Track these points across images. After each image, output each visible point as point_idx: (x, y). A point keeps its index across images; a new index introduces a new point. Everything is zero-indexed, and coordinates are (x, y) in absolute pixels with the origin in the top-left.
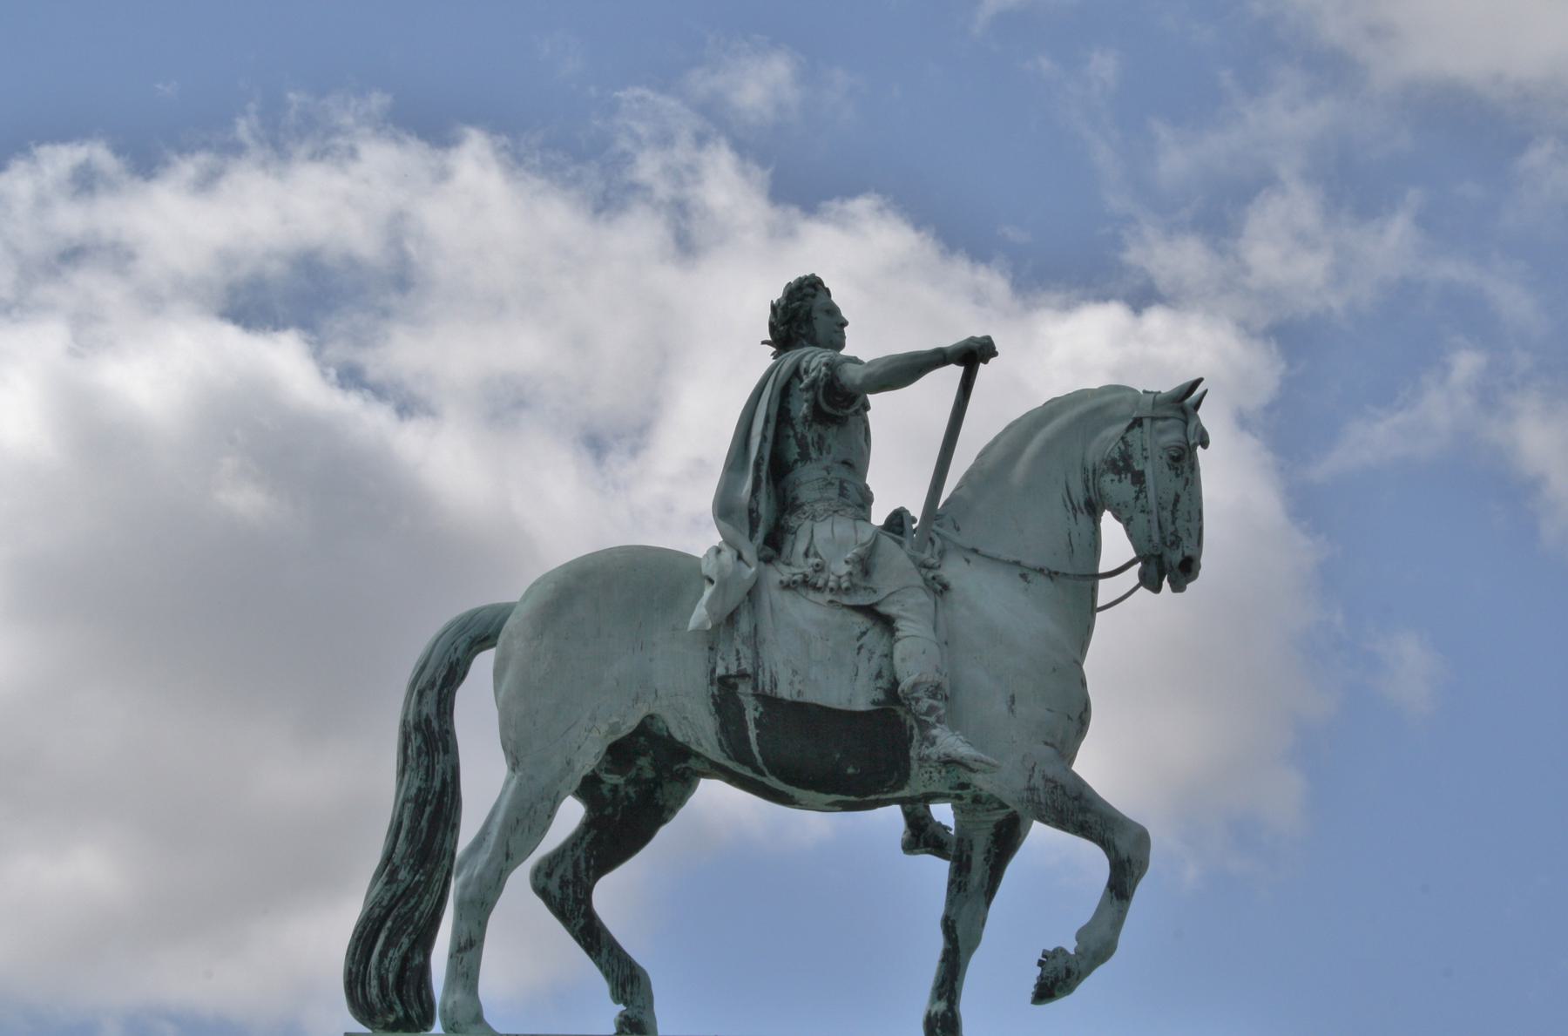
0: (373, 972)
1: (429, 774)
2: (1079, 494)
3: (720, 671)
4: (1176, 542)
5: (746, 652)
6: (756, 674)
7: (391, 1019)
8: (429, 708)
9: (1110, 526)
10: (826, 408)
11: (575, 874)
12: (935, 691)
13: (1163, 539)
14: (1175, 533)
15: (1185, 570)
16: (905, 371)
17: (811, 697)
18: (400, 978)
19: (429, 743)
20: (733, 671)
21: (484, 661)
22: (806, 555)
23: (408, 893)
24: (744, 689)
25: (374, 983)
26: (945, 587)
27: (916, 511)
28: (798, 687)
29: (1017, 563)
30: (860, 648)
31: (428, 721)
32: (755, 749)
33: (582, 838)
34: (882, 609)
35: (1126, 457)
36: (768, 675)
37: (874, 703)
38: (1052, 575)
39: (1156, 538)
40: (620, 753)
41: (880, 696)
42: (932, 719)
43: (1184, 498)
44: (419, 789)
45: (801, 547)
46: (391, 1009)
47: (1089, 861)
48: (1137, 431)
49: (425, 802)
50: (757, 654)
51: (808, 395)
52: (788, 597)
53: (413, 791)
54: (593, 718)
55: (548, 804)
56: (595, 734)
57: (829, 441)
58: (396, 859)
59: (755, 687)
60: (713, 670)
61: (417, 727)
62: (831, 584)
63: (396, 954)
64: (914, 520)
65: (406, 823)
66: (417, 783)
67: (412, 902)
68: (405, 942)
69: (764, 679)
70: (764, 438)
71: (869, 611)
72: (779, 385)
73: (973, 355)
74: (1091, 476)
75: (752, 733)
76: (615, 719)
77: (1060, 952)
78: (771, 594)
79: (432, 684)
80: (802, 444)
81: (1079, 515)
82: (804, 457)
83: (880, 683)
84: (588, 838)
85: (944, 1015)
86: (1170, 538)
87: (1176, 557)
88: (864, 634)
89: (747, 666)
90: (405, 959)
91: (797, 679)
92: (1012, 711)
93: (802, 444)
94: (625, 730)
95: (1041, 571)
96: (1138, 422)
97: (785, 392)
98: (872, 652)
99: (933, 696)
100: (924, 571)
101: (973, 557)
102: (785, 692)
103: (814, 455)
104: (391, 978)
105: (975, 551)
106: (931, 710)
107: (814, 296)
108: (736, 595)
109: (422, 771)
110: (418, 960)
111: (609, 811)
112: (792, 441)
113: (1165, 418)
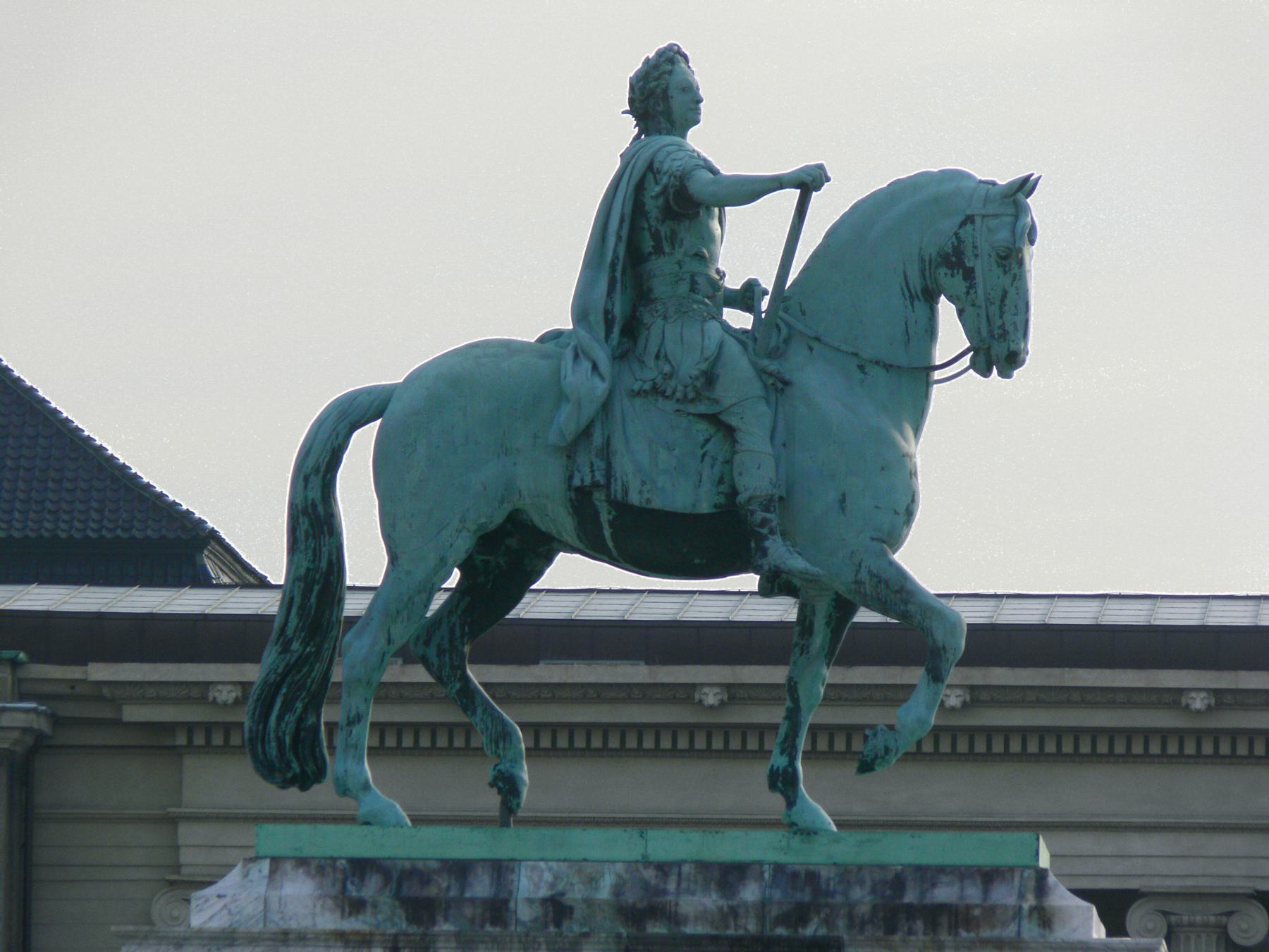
0: (272, 735)
1: (316, 555)
2: (916, 282)
4: (1004, 335)
5: (600, 464)
7: (289, 775)
8: (315, 494)
9: (946, 309)
10: (675, 207)
11: (451, 642)
13: (991, 332)
14: (1002, 327)
15: (1010, 361)
16: (750, 190)
17: (657, 504)
20: (588, 481)
21: (364, 441)
22: (657, 357)
23: (303, 660)
24: (599, 496)
25: (273, 744)
26: (787, 383)
27: (768, 283)
28: (646, 496)
29: (856, 355)
30: (704, 455)
31: (314, 505)
32: (610, 544)
33: (457, 606)
34: (724, 418)
35: (958, 251)
36: (619, 483)
37: (715, 506)
38: (888, 367)
40: (488, 540)
41: (721, 500)
42: (765, 531)
43: (1012, 291)
44: (308, 570)
46: (289, 767)
48: (969, 227)
49: (314, 581)
51: (661, 201)
53: (303, 571)
54: (463, 520)
55: (424, 596)
56: (464, 534)
57: (682, 235)
58: (290, 632)
59: (608, 496)
60: (571, 478)
61: (305, 512)
62: (679, 395)
63: (291, 718)
64: (765, 292)
65: (297, 600)
66: (305, 564)
67: (305, 670)
68: (299, 706)
69: (617, 488)
70: (619, 237)
71: (713, 419)
72: (633, 182)
73: (808, 183)
74: (928, 267)
75: (607, 532)
76: (483, 520)
79: (317, 471)
80: (656, 236)
81: (916, 303)
82: (658, 250)
83: (722, 488)
84: (463, 606)
85: (785, 770)
86: (997, 332)
88: (707, 441)
89: (600, 477)
90: (300, 720)
91: (645, 488)
93: (656, 236)
94: (491, 527)
95: (877, 363)
96: (969, 219)
97: (640, 187)
98: (714, 459)
99: (767, 510)
100: (764, 376)
101: (815, 345)
102: (635, 499)
103: (667, 249)
104: (288, 739)
105: (818, 339)
106: (764, 522)
107: (670, 73)
108: (589, 411)
109: (310, 552)
110: (311, 720)
111: (481, 579)
112: (647, 234)
113: (996, 216)
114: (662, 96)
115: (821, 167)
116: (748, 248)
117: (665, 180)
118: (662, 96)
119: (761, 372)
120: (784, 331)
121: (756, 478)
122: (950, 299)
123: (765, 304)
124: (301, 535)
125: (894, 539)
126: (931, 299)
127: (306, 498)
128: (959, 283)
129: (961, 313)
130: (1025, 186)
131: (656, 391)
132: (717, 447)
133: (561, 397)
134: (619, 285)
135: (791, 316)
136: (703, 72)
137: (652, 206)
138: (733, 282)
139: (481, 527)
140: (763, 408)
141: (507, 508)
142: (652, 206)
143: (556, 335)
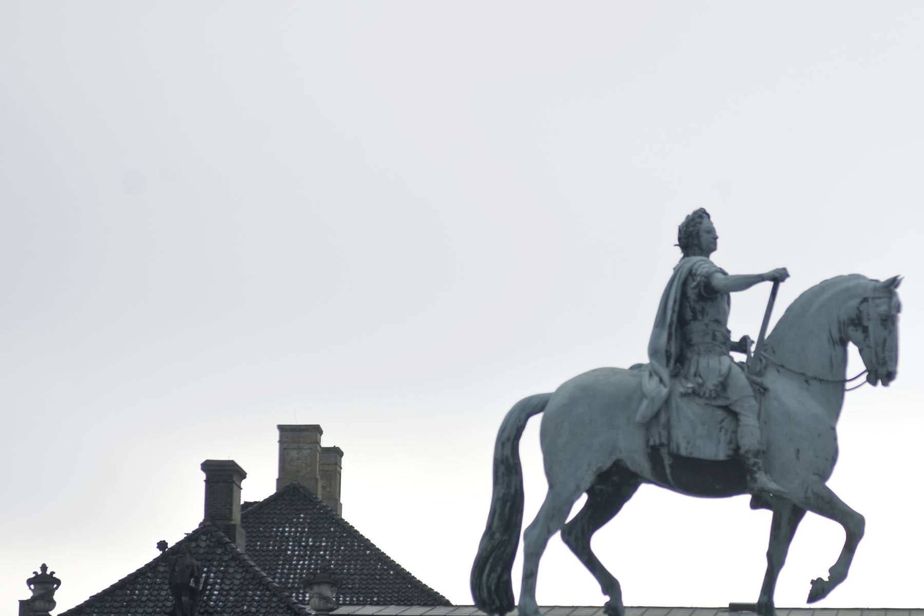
0: (484, 585)
1: (509, 486)
3: (651, 443)
4: (885, 363)
6: (669, 445)
7: (494, 607)
8: (508, 452)
9: (853, 350)
10: (704, 294)
12: (757, 454)
13: (878, 363)
14: (884, 358)
17: (697, 454)
18: (497, 587)
19: (507, 469)
20: (658, 442)
21: (534, 424)
22: (695, 375)
24: (664, 451)
25: (485, 590)
26: (766, 389)
27: (754, 337)
29: (803, 374)
30: (721, 428)
31: (507, 459)
34: (733, 408)
37: (728, 456)
38: (821, 381)
39: (874, 361)
40: (603, 477)
41: (731, 453)
42: (755, 469)
45: (692, 371)
46: (493, 603)
47: (836, 533)
48: (865, 304)
50: (669, 434)
51: (696, 290)
52: (685, 399)
53: (501, 495)
54: (589, 465)
56: (590, 472)
58: (494, 528)
59: (669, 450)
60: (648, 441)
61: (502, 462)
62: (707, 395)
64: (753, 342)
65: (498, 511)
66: (503, 491)
68: (499, 569)
69: (673, 446)
70: (674, 311)
71: (726, 409)
72: (681, 281)
73: (778, 278)
74: (842, 326)
75: (668, 471)
76: (600, 465)
77: (820, 579)
78: (677, 401)
79: (508, 439)
80: (693, 310)
81: (837, 347)
82: (695, 318)
86: (881, 361)
87: (882, 371)
88: (723, 420)
89: (664, 440)
90: (500, 577)
92: (797, 457)
93: (693, 310)
94: (605, 468)
95: (816, 378)
96: (865, 300)
97: (685, 284)
99: (756, 456)
101: (780, 369)
102: (683, 452)
103: (699, 317)
104: (493, 588)
105: (782, 366)
106: (755, 464)
107: (700, 223)
108: (658, 404)
110: (505, 577)
112: (688, 310)
113: (879, 298)
114: (696, 235)
115: (784, 269)
116: (745, 317)
117: (699, 279)
118: (696, 235)
119: (753, 383)
120: (764, 361)
121: (750, 438)
122: (855, 343)
123: (753, 348)
124: (500, 474)
125: (825, 474)
126: (844, 344)
127: (503, 454)
128: (859, 334)
129: (861, 351)
130: (894, 282)
131: (694, 393)
132: (728, 423)
133: (643, 396)
134: (673, 337)
135: (769, 352)
136: (718, 221)
137: (692, 294)
138: (735, 338)
139: (599, 468)
140: (753, 402)
141: (614, 458)
142: (692, 294)
143: (638, 367)
